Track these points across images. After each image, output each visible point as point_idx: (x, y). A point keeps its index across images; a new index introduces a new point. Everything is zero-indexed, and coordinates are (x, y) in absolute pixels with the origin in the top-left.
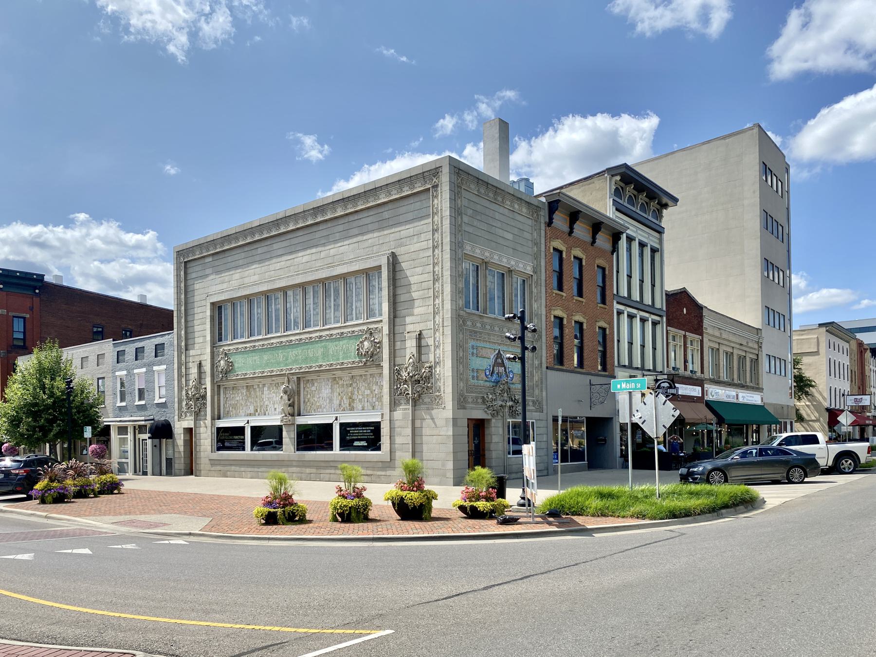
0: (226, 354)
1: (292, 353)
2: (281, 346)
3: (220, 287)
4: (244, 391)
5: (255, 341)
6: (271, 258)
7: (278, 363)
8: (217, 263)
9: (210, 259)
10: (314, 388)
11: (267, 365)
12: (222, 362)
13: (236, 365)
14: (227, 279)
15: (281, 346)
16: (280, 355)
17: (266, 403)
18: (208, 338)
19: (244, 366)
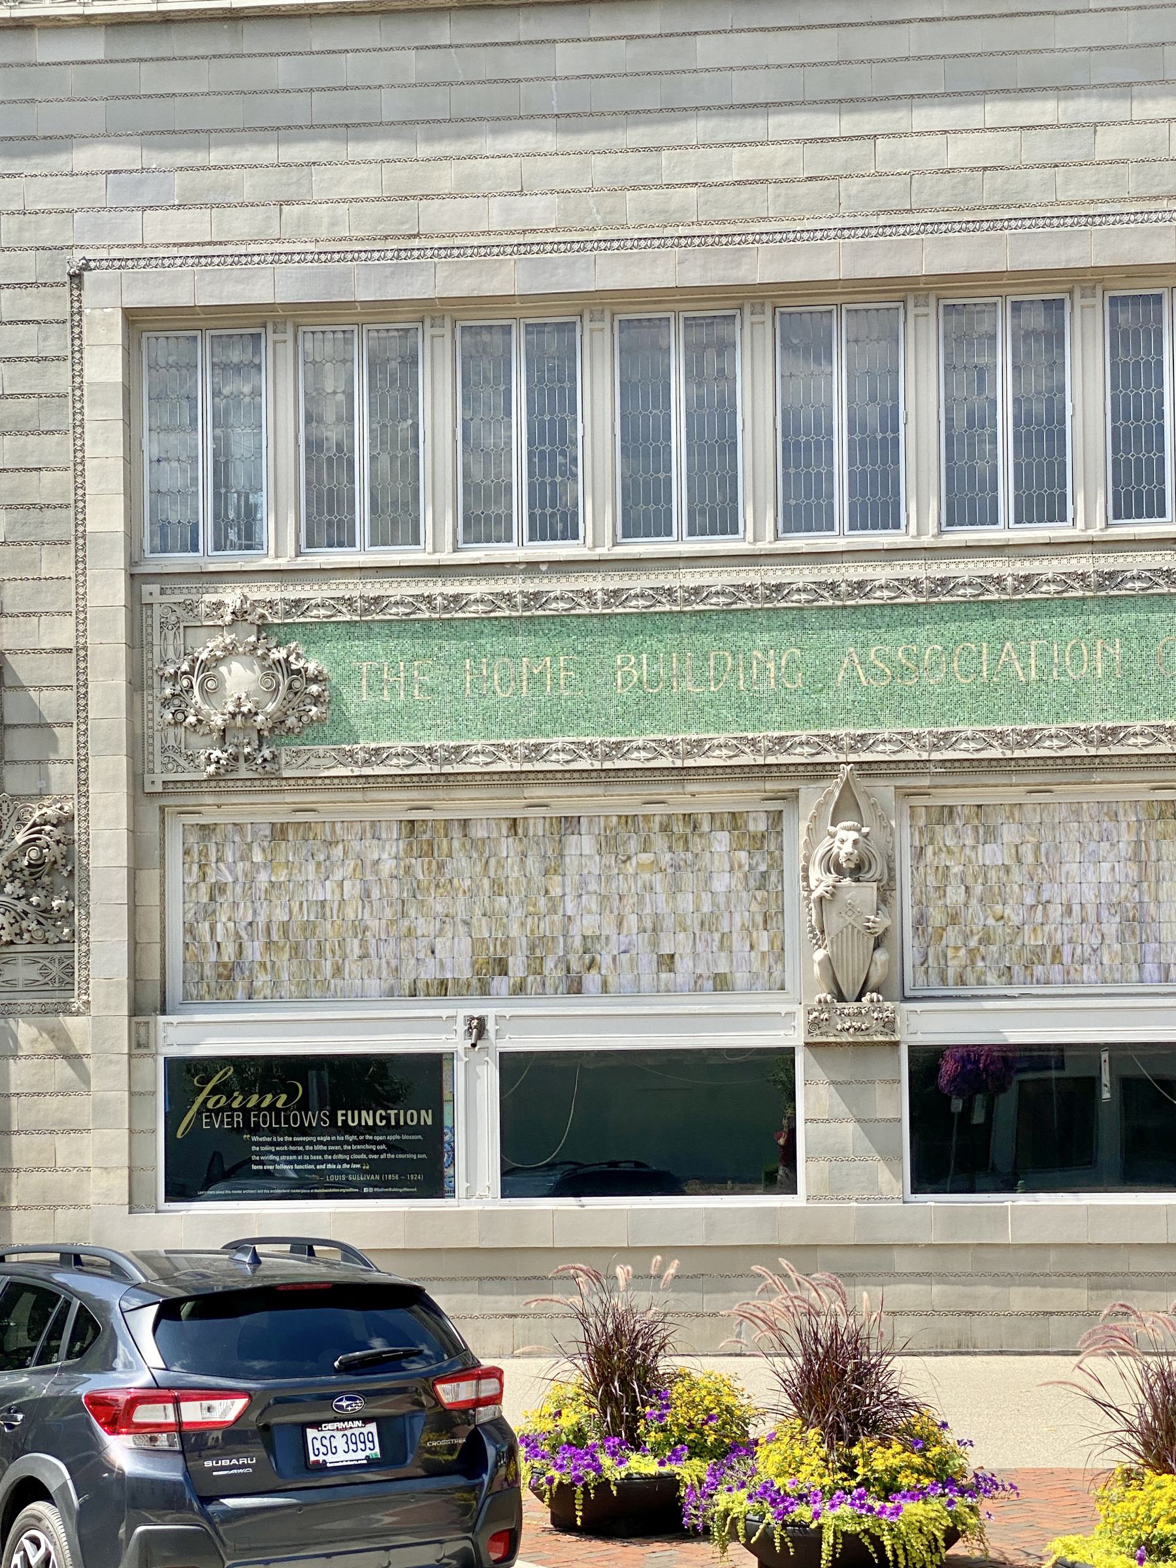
0: (263, 628)
1: (860, 659)
2: (769, 611)
3: (195, 225)
4: (387, 854)
5: (532, 567)
6: (671, 112)
7: (746, 707)
8: (150, 79)
9: (94, 47)
10: (992, 854)
11: (644, 709)
12: (240, 679)
13: (357, 700)
14: (250, 185)
15: (769, 611)
16: (769, 658)
17: (588, 924)
18: (107, 517)
19: (392, 704)
